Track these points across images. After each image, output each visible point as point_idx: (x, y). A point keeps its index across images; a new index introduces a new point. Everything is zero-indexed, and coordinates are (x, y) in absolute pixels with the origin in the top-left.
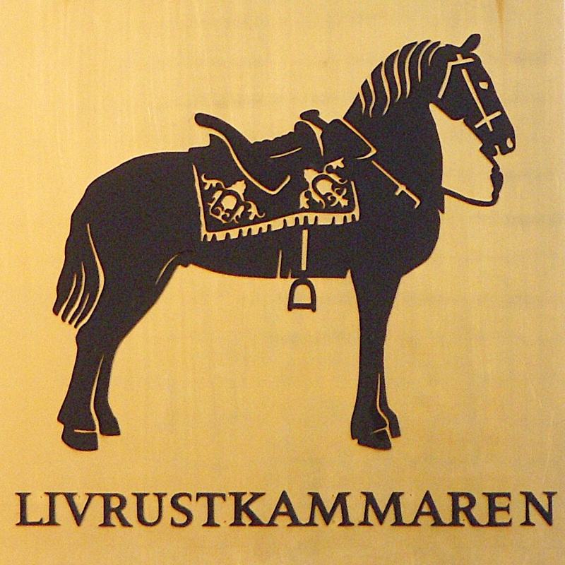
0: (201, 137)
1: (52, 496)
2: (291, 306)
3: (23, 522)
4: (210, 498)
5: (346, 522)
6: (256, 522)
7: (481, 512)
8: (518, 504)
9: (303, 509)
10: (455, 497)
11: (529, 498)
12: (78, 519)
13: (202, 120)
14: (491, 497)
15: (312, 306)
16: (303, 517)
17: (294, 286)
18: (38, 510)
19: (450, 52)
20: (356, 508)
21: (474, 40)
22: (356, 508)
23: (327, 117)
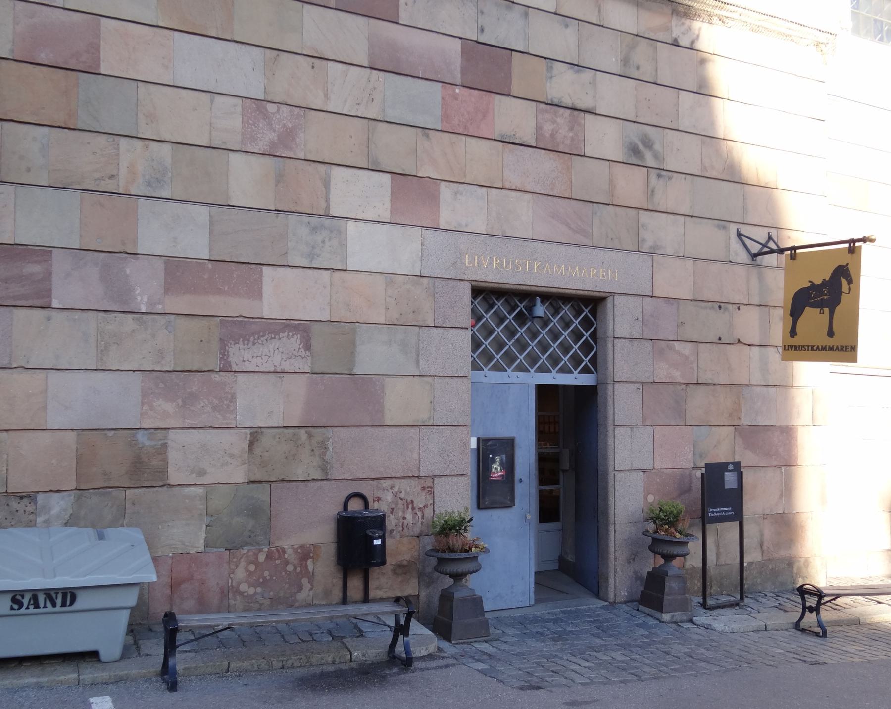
0: (809, 284)
1: (788, 346)
2: (820, 313)
3: (785, 350)
4: (808, 346)
5: (826, 351)
6: (814, 350)
7: (845, 349)
8: (850, 347)
9: (820, 348)
10: (841, 346)
11: (852, 347)
12: (791, 350)
13: (810, 281)
14: (846, 346)
15: (823, 313)
16: (820, 349)
17: (821, 310)
18: (786, 349)
19: (845, 266)
20: (827, 348)
21: (848, 264)
22: (827, 348)
23: (826, 280)
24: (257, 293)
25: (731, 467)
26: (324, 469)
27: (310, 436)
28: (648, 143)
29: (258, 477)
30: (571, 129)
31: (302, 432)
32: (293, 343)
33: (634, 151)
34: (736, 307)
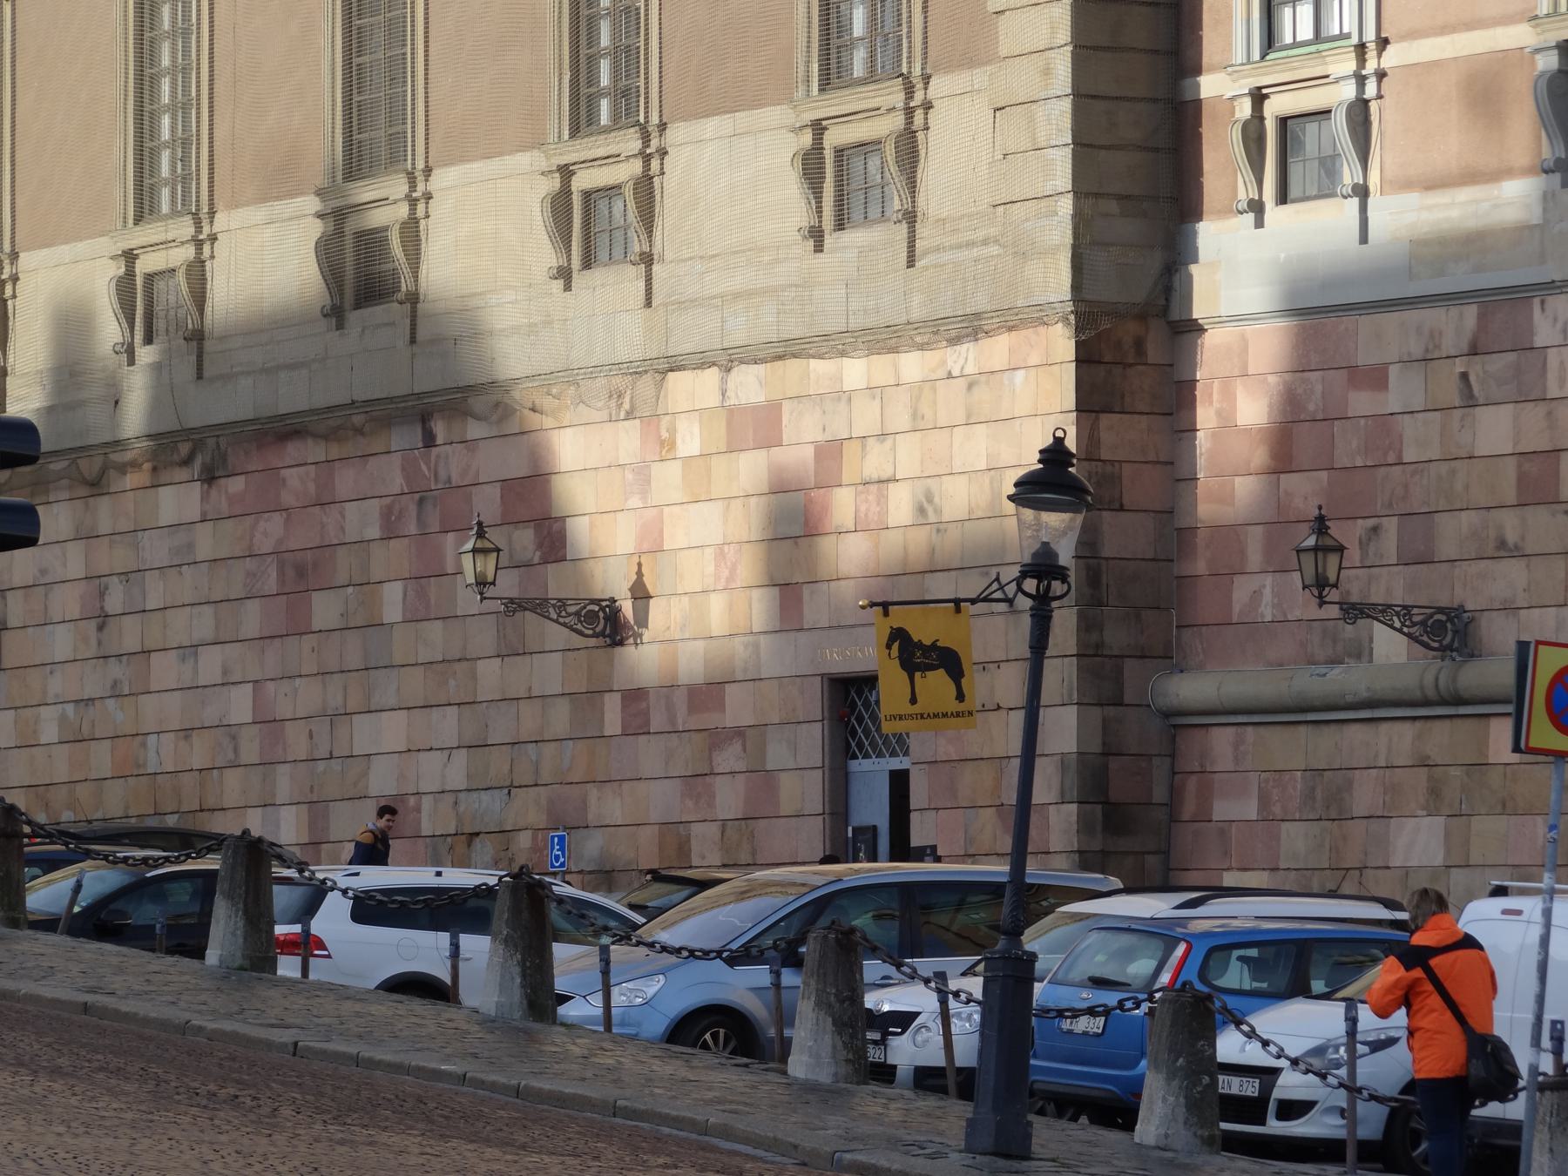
24: (721, 707)
25: (928, 851)
26: (754, 853)
27: (747, 826)
28: (929, 498)
29: (726, 862)
30: (878, 504)
31: (743, 822)
32: (737, 747)
33: (922, 511)
34: (996, 665)
